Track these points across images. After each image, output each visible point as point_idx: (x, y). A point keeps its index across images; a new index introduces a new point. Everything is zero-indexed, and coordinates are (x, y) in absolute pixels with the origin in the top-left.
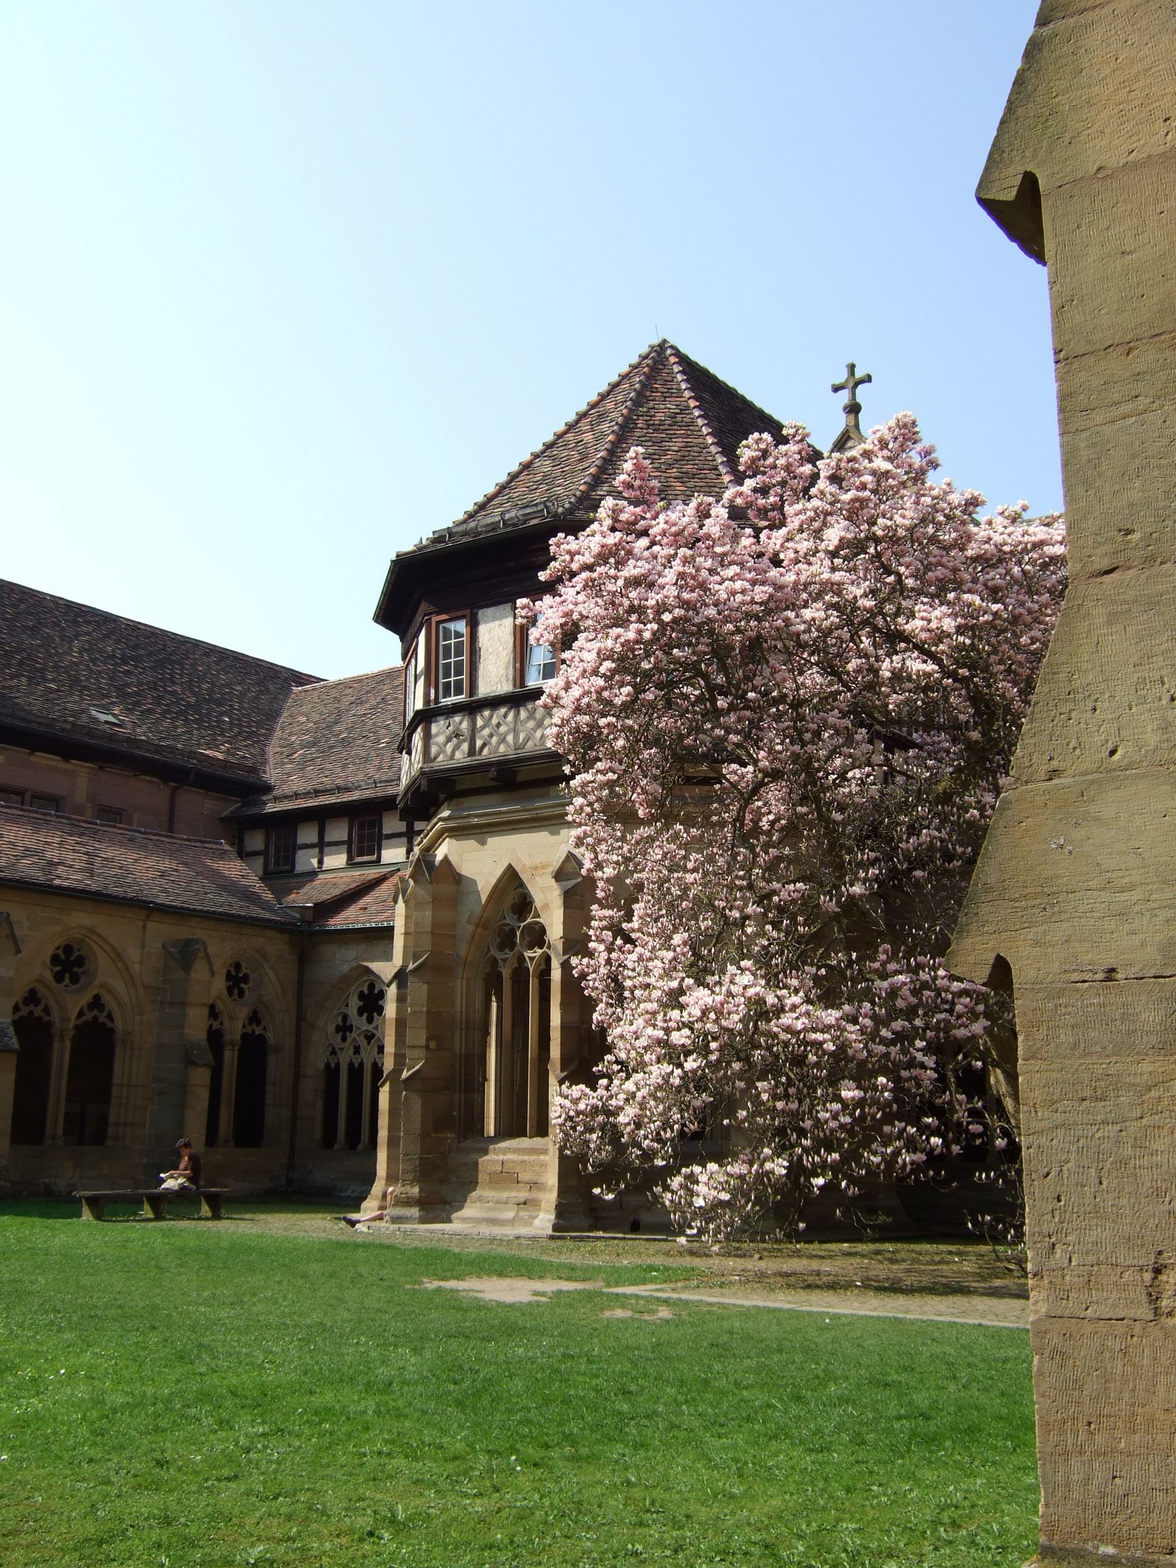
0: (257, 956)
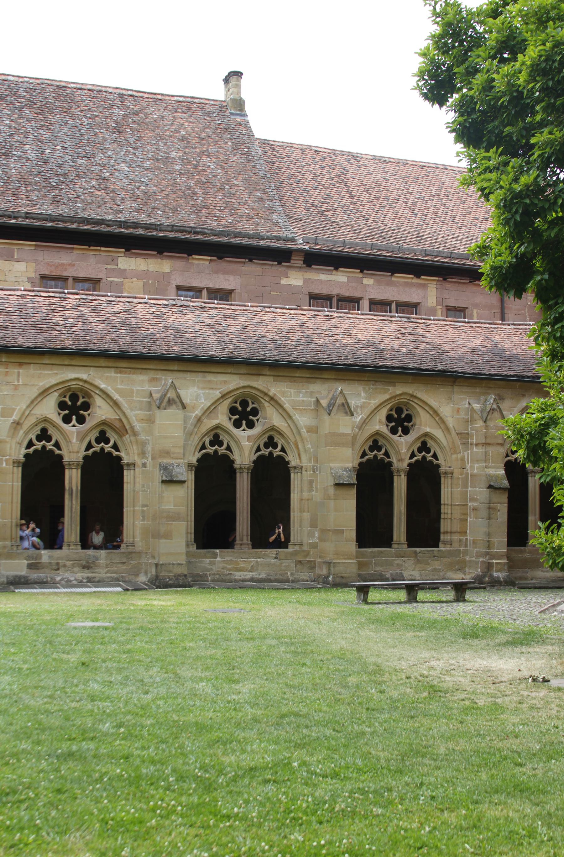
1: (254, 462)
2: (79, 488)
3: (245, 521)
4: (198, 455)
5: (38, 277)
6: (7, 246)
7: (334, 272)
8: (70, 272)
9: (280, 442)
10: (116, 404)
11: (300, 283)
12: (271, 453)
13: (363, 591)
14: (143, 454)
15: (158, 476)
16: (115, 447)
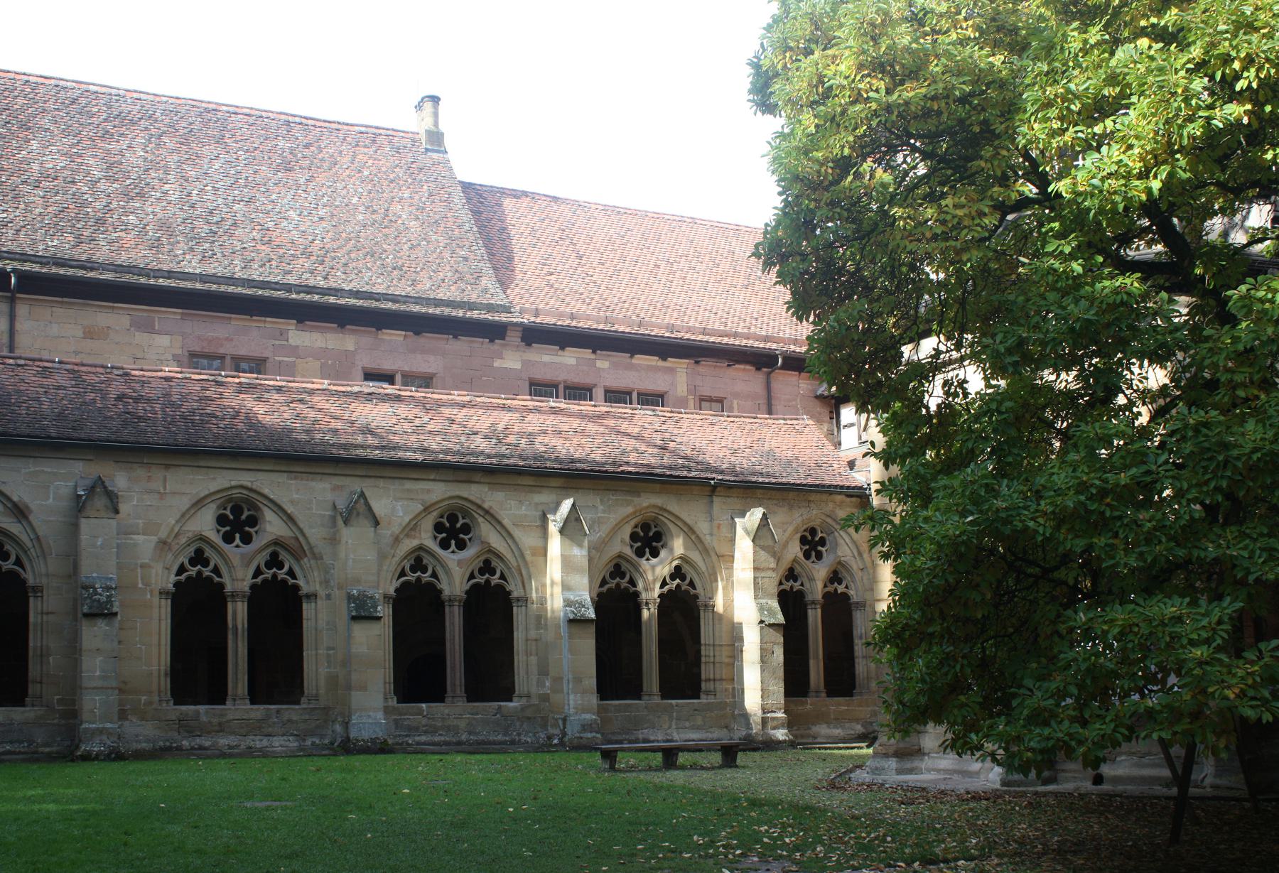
0: (829, 520)
1: (467, 593)
2: (246, 626)
4: (396, 584)
5: (187, 354)
6: (145, 314)
7: (560, 353)
8: (227, 349)
9: (499, 567)
10: (290, 519)
11: (518, 366)
12: (488, 581)
13: (609, 756)
14: (326, 583)
15: (344, 610)
16: (291, 573)
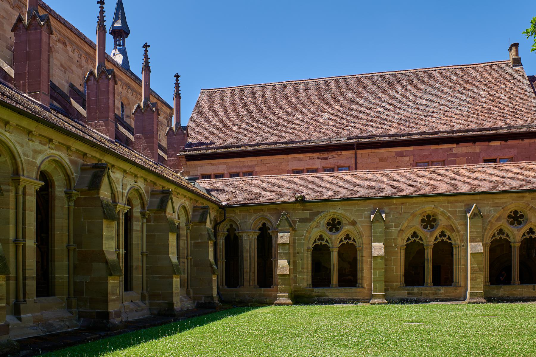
2: (432, 258)
3: (517, 271)
